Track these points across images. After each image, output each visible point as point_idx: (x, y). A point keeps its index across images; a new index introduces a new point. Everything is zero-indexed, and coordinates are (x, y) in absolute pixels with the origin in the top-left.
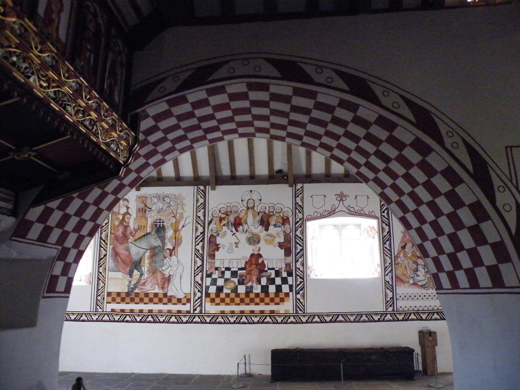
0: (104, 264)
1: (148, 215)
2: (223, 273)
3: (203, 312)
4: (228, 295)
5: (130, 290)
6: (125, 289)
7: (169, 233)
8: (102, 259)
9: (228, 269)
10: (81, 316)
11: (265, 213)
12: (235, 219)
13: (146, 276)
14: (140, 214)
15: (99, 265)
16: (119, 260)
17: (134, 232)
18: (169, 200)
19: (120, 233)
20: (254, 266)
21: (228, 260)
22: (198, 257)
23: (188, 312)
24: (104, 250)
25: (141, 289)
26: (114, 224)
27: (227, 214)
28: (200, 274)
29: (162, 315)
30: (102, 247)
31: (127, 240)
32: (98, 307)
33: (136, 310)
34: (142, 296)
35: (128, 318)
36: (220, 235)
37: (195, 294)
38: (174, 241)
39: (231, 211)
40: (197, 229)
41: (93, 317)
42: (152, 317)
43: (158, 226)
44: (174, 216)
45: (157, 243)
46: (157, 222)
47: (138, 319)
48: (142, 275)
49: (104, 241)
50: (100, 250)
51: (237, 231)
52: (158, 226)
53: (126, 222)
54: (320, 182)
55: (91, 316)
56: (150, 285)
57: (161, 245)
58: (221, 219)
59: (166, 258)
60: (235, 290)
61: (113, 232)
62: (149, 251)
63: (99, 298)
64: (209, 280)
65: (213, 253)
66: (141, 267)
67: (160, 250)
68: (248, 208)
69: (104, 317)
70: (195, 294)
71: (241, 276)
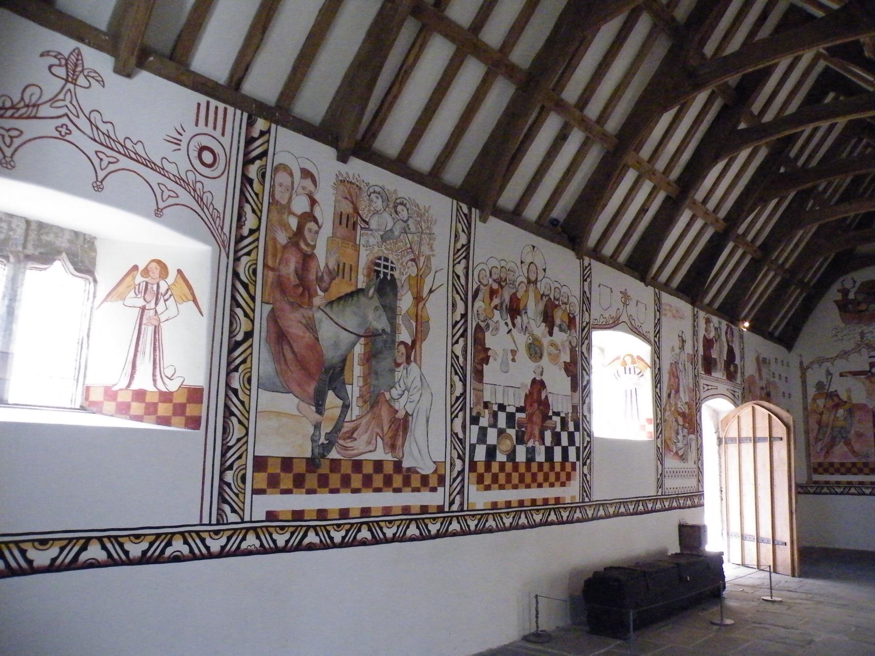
0: (244, 361)
1: (362, 238)
2: (495, 415)
3: (465, 508)
4: (502, 465)
5: (317, 451)
6: (299, 447)
7: (405, 302)
8: (238, 344)
9: (502, 407)
10: (169, 544)
11: (550, 298)
12: (511, 299)
13: (355, 411)
14: (342, 231)
15: (229, 364)
16: (289, 355)
17: (326, 278)
18: (404, 214)
19: (290, 268)
20: (536, 405)
21: (501, 389)
22: (456, 373)
23: (440, 509)
24: (246, 315)
25: (346, 448)
26: (274, 239)
27: (499, 282)
28: (461, 414)
29: (390, 522)
30: (239, 305)
31: (311, 297)
32: (227, 508)
33: (333, 511)
34: (346, 468)
35: (312, 538)
36: (491, 328)
37: (452, 465)
38: (414, 324)
39: (506, 280)
40: (454, 305)
41: (209, 542)
42: (370, 530)
43: (382, 276)
44: (413, 260)
45: (380, 323)
46: (378, 265)
47: (338, 536)
48: (346, 407)
49: (245, 286)
50: (233, 315)
51: (514, 325)
52: (382, 276)
53: (307, 244)
54: (604, 263)
55: (203, 541)
56: (365, 437)
57: (388, 330)
58: (493, 293)
59: (398, 365)
60: (511, 456)
61: (270, 263)
62: (362, 340)
63: (229, 476)
64: (475, 429)
65: (479, 367)
66: (344, 383)
67: (386, 342)
68: (529, 282)
69: (244, 539)
70: (452, 465)
71: (520, 426)
